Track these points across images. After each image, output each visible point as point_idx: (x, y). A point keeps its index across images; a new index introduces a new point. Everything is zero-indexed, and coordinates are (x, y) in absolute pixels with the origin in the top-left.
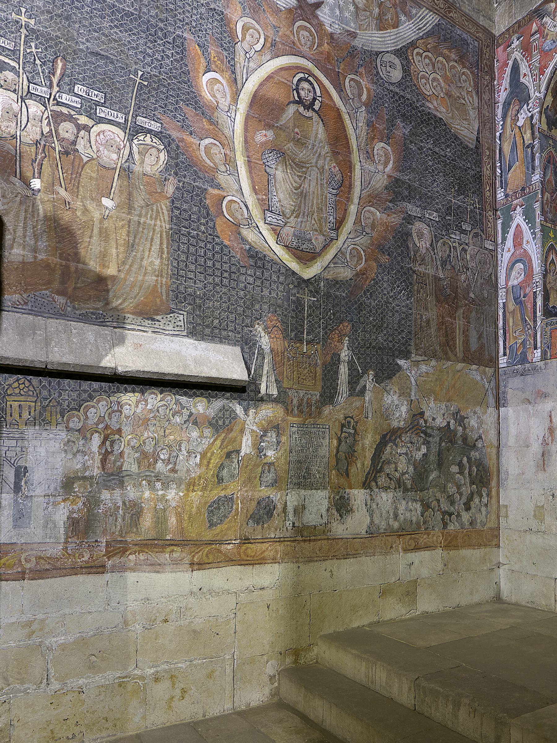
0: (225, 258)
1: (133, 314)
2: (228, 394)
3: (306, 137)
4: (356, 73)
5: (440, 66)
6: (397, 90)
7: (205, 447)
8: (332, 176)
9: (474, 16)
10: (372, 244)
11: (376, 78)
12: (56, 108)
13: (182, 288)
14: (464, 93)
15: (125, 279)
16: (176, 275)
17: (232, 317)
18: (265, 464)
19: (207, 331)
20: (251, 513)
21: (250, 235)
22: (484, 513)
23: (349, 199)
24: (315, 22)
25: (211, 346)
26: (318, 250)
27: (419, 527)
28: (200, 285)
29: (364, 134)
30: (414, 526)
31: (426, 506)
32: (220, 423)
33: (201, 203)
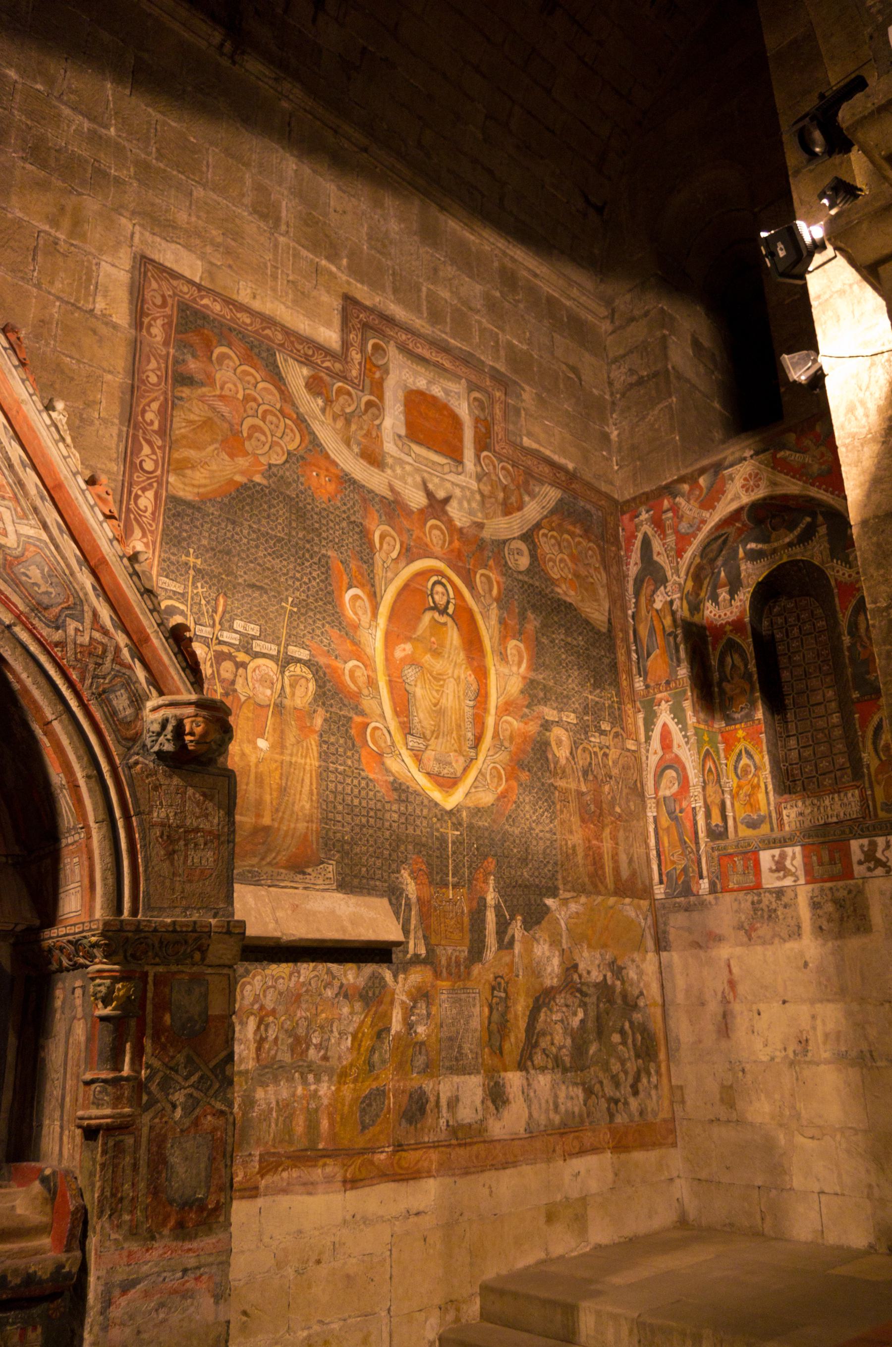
0: (371, 793)
1: (285, 868)
2: (378, 958)
3: (442, 645)
4: (486, 566)
5: (565, 544)
6: (526, 579)
7: (356, 1025)
8: (468, 685)
9: (596, 484)
10: (511, 760)
11: (505, 569)
12: (219, 648)
13: (331, 834)
14: (592, 571)
15: (279, 829)
16: (325, 820)
17: (379, 863)
18: (416, 1043)
19: (356, 882)
20: (403, 1109)
21: (392, 763)
22: (654, 1097)
23: (486, 710)
24: (445, 519)
25: (361, 900)
26: (459, 774)
27: (582, 1122)
28: (347, 829)
29: (496, 633)
30: (577, 1119)
31: (589, 1092)
32: (370, 994)
33: (347, 736)
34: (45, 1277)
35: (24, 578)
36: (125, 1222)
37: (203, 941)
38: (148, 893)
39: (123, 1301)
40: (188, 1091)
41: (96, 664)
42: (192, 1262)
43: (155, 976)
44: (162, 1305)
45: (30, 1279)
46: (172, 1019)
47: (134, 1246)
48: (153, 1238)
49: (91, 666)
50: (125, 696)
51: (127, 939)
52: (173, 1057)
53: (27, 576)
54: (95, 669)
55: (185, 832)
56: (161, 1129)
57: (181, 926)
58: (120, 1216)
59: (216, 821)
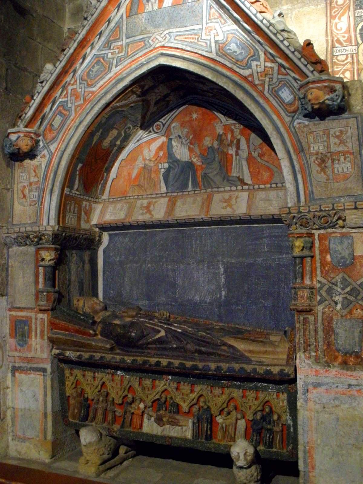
34: (274, 373)
35: (229, 51)
36: (313, 356)
37: (340, 214)
38: (312, 192)
39: (315, 391)
40: (345, 296)
41: (269, 78)
42: (354, 382)
43: (319, 235)
44: (336, 398)
45: (269, 372)
46: (332, 258)
47: (318, 368)
48: (329, 366)
49: (267, 80)
50: (287, 90)
51: (294, 217)
52: (333, 278)
53: (231, 50)
54: (269, 81)
55: (331, 155)
56: (329, 315)
57: (325, 207)
58: (310, 353)
59: (350, 145)
